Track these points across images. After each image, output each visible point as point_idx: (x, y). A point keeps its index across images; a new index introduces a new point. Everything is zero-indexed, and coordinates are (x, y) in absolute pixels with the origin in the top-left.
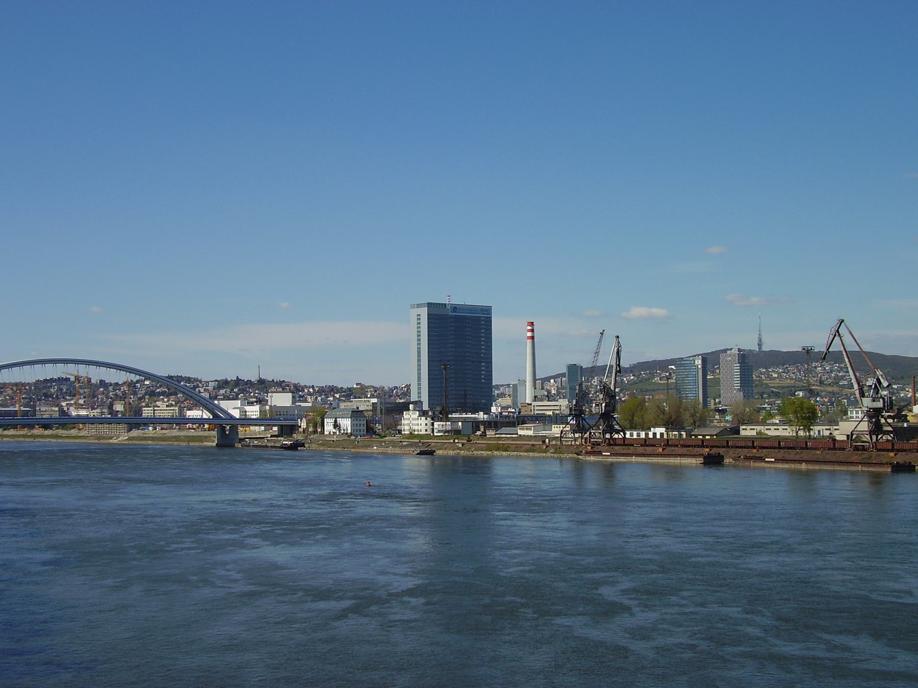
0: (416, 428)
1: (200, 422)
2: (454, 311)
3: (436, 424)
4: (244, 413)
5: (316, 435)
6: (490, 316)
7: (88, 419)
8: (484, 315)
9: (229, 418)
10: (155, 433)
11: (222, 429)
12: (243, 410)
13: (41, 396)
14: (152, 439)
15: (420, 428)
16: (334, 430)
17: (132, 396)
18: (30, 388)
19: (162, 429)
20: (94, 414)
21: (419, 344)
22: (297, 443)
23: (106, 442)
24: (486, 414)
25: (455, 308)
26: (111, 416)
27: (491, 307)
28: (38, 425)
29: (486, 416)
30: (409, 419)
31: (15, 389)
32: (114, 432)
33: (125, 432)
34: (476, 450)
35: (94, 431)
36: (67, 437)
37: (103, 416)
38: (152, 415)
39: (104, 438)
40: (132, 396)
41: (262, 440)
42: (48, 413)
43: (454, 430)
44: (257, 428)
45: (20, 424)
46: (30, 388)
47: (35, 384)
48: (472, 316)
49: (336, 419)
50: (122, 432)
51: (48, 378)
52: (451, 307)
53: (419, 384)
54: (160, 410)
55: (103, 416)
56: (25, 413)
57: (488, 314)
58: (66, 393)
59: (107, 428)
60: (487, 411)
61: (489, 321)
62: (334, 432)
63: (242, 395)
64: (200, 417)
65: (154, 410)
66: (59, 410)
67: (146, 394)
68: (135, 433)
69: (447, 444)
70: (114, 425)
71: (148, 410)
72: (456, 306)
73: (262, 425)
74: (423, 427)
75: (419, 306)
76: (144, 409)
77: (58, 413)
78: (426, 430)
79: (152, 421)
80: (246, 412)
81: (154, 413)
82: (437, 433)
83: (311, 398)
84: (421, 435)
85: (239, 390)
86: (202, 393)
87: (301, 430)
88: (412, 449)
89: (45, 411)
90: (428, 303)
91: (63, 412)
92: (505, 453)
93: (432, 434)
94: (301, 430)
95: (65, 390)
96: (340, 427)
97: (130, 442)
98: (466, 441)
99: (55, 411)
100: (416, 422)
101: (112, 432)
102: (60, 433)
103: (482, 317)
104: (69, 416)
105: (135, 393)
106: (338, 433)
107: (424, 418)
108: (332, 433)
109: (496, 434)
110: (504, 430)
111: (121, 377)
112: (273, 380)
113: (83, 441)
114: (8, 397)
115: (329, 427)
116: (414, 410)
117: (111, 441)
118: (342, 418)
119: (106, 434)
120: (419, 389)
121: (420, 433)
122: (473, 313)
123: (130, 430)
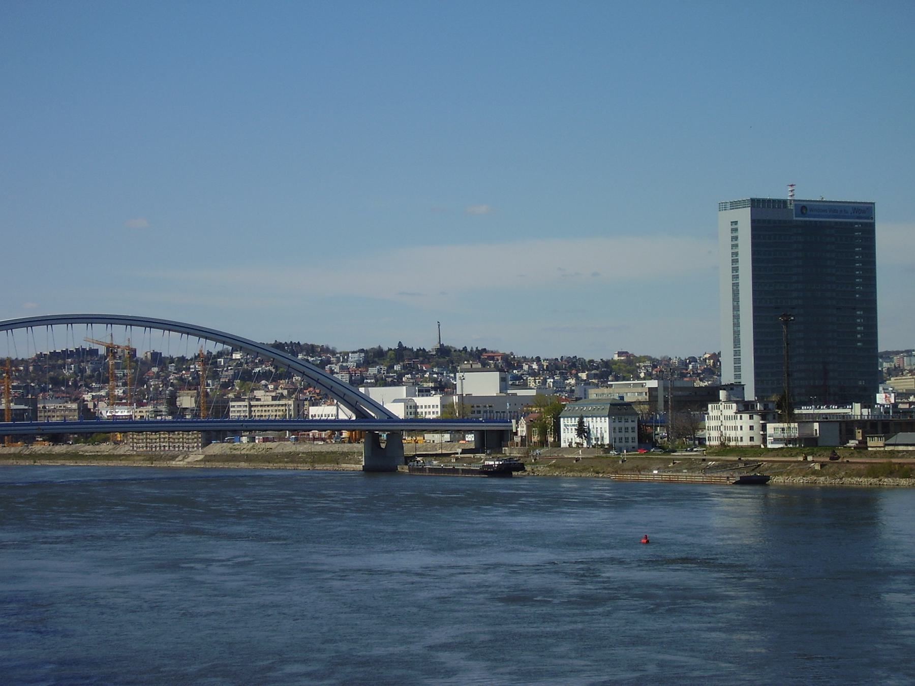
0: (732, 434)
1: (333, 426)
2: (802, 213)
3: (770, 427)
4: (413, 410)
5: (545, 449)
6: (871, 221)
8: (861, 221)
10: (253, 448)
11: (374, 440)
12: (410, 404)
13: (46, 384)
14: (248, 458)
15: (739, 433)
16: (578, 440)
17: (210, 382)
18: (26, 369)
19: (266, 440)
21: (736, 277)
23: (164, 464)
24: (865, 408)
25: (803, 208)
26: (173, 418)
27: (874, 203)
28: (42, 435)
29: (865, 412)
30: (718, 418)
32: (179, 447)
33: (197, 447)
34: (849, 475)
35: (141, 445)
36: (95, 457)
37: (159, 418)
38: (247, 414)
39: (160, 458)
40: (210, 382)
41: (446, 459)
42: (58, 414)
43: (805, 439)
44: (436, 437)
45: (8, 435)
46: (26, 369)
47: (34, 360)
48: (836, 223)
49: (581, 418)
50: (193, 447)
51: (57, 351)
52: (796, 205)
53: (737, 353)
54: (261, 406)
55: (159, 418)
56: (19, 414)
57: (868, 218)
58: (91, 377)
59: (166, 440)
60: (868, 401)
61: (869, 232)
62: (578, 444)
63: (409, 376)
64: (334, 418)
65: (251, 406)
66: (79, 408)
67: (235, 377)
68: (216, 448)
69: (793, 464)
70: (179, 434)
72: (805, 203)
73: (446, 431)
74: (746, 434)
75: (735, 205)
76: (232, 404)
77: (76, 413)
78: (752, 439)
79: (247, 426)
80: (416, 407)
81: (250, 411)
82: (772, 443)
83: (535, 379)
84: (742, 447)
85: (404, 367)
86: (337, 373)
87: (517, 439)
88: (725, 475)
89: (54, 410)
90: (753, 200)
91: (84, 411)
92: (904, 482)
93: (762, 446)
94: (517, 439)
95: (88, 372)
96: (589, 433)
97: (208, 465)
98: (828, 459)
99: (71, 410)
100: (731, 423)
101: (174, 447)
102: (82, 449)
103: (856, 223)
104: (98, 418)
105: (215, 376)
106: (585, 445)
107: (748, 415)
108: (574, 445)
109: (886, 445)
110: (901, 437)
111: (189, 347)
112: (465, 349)
113: (124, 463)
115: (569, 434)
116: (729, 400)
117: (174, 463)
118: (592, 417)
119: (164, 450)
120: (737, 361)
121: (740, 444)
122: (836, 217)
123: (207, 443)
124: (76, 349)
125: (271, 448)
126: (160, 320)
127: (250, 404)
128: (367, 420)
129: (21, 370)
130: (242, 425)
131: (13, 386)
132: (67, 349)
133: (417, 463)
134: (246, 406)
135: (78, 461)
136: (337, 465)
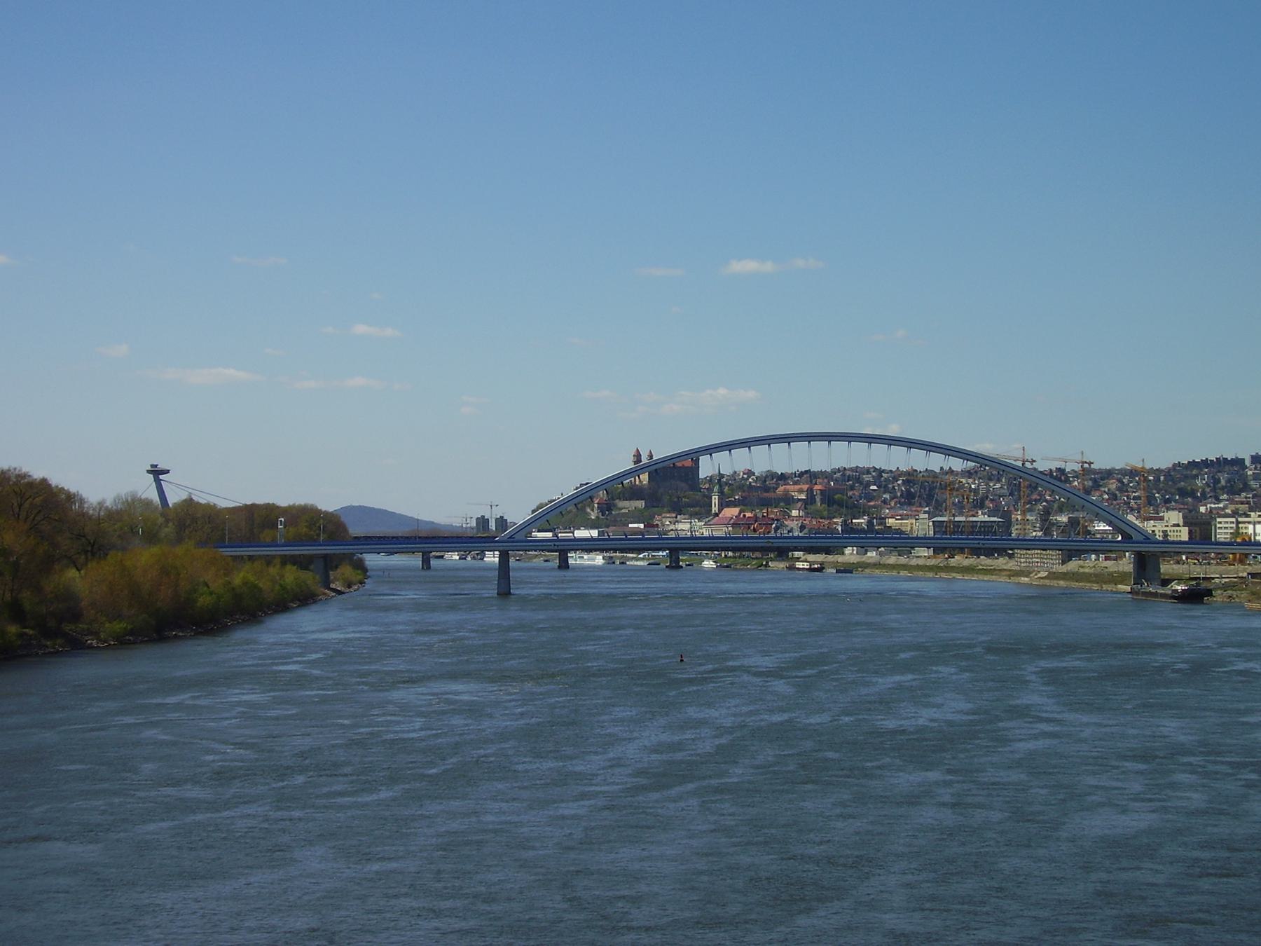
7: (925, 539)
9: (1141, 538)
18: (1157, 479)
19: (1106, 559)
20: (1153, 529)
22: (1195, 589)
26: (1045, 534)
31: (1125, 481)
45: (967, 548)
46: (1157, 479)
47: (1169, 470)
51: (1197, 460)
58: (1223, 488)
65: (1238, 523)
68: (1073, 565)
71: (1227, 522)
76: (1218, 520)
81: (1238, 528)
95: (1223, 482)
102: (983, 563)
114: (1106, 496)
124: (1216, 458)
125: (1106, 568)
126: (752, 438)
127: (1237, 520)
128: (1131, 541)
129: (1150, 481)
130: (979, 543)
131: (1134, 497)
132: (1207, 459)
133: (1141, 586)
134: (1233, 522)
135: (965, 575)
136: (1114, 586)
